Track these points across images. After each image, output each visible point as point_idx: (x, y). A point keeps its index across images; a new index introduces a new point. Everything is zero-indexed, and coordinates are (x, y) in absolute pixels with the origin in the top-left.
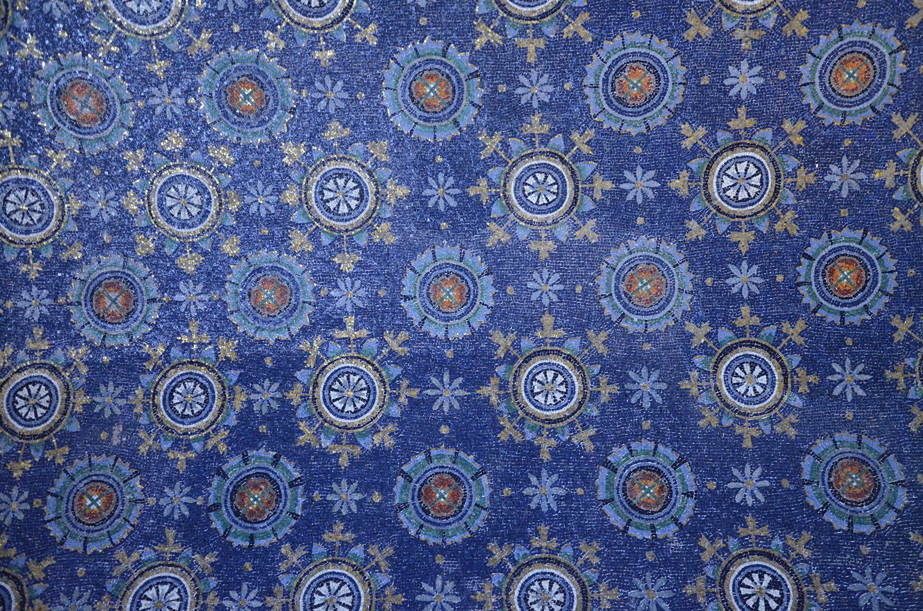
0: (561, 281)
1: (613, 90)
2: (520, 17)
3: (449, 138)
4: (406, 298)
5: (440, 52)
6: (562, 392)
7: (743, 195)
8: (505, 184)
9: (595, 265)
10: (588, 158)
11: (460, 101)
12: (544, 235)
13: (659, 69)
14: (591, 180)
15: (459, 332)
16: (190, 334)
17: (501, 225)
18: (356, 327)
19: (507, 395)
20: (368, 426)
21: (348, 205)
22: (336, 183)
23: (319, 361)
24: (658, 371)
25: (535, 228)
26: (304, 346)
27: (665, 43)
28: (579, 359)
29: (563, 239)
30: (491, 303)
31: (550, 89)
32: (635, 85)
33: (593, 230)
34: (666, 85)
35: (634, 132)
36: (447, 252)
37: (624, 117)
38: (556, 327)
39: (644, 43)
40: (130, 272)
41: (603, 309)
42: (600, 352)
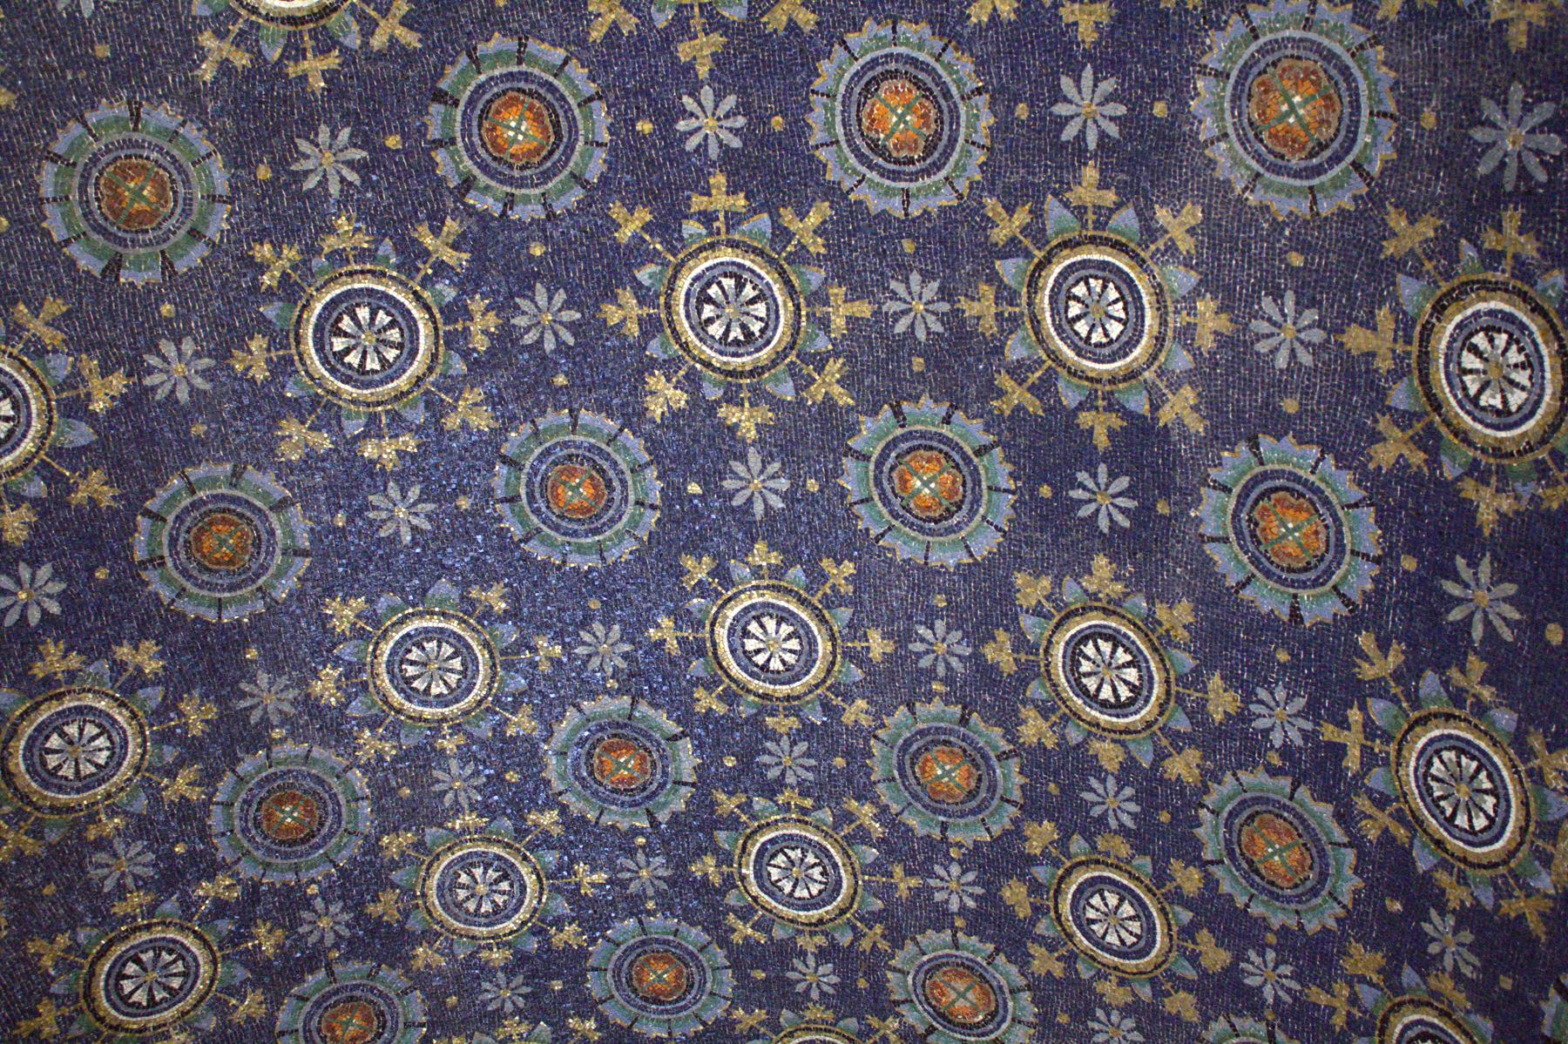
0: (1278, 295)
1: (911, 161)
2: (796, 329)
3: (1009, 467)
5: (861, 464)
6: (1509, 344)
8: (1088, 379)
9: (1246, 217)
10: (1038, 213)
12: (1184, 319)
13: (870, 74)
14: (1080, 211)
15: (1364, 531)
16: (1333, 1010)
18: (1343, 724)
19: (1503, 473)
20: (1528, 785)
23: (1399, 817)
24: (1484, 101)
25: (1170, 333)
27: (824, 66)
28: (1445, 287)
29: (1194, 277)
31: (915, 278)
32: (901, 118)
33: (1176, 213)
34: (897, 58)
35: (987, 120)
36: (1212, 512)
37: (961, 140)
39: (825, 106)
41: (1342, 211)
42: (1431, 234)
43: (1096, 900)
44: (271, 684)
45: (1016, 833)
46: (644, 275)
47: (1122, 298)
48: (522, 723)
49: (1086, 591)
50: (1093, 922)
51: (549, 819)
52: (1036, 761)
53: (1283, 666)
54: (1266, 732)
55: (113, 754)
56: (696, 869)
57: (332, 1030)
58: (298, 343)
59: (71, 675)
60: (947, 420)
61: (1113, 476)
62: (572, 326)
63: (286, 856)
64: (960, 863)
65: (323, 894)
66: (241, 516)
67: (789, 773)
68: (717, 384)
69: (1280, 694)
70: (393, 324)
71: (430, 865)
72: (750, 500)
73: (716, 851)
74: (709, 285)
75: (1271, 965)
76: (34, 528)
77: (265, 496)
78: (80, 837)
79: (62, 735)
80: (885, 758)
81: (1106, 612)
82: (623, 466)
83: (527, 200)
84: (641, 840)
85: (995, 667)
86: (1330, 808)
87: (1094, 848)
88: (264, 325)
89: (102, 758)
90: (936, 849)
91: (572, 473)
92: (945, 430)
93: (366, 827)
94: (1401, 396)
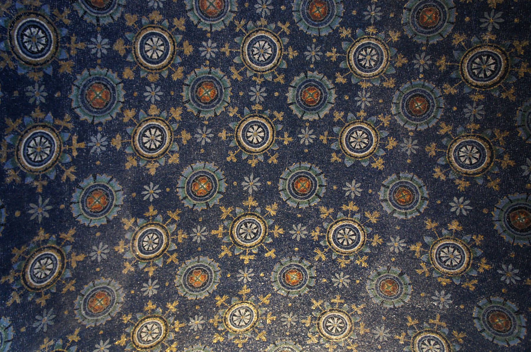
3: (178, 194)
4: (95, 178)
7: (143, 335)
10: (165, 262)
11: (195, 199)
15: (76, 210)
17: (134, 224)
21: (147, 142)
22: (159, 136)
23: (58, 127)
26: (67, 117)
28: (59, 279)
29: (125, 257)
30: (92, 225)
31: (199, 241)
33: (129, 271)
36: (120, 199)
38: (78, 262)
40: (115, 7)
41: (87, 285)
43: (160, 54)
44: (407, 150)
45: (185, 73)
46: (270, 240)
47: (144, 247)
48: (338, 116)
49: (158, 162)
50: (162, 45)
51: (340, 79)
52: (177, 102)
53: (98, 160)
54: (103, 136)
55: (460, 149)
56: (296, 54)
57: (436, 17)
58: (364, 241)
59: (460, 178)
60: (194, 205)
61: (149, 199)
62: (292, 229)
63: (425, 92)
64: (206, 59)
65: (419, 73)
66: (396, 201)
67: (258, 90)
68: (257, 212)
69: (99, 150)
70: (339, 239)
71: (382, 72)
72: (254, 179)
73: (288, 61)
74: (254, 238)
75: (99, 51)
76: (450, 222)
77: (388, 205)
78: (482, 127)
79: (471, 162)
80: (226, 96)
81: (152, 158)
82: (288, 190)
83: (296, 261)
84: (312, 66)
85: (188, 132)
86: (81, 119)
87: (160, 74)
88: (371, 247)
89: (464, 149)
90: (213, 63)
91: (303, 191)
92: (195, 202)
93: (397, 93)
94: (69, 248)
